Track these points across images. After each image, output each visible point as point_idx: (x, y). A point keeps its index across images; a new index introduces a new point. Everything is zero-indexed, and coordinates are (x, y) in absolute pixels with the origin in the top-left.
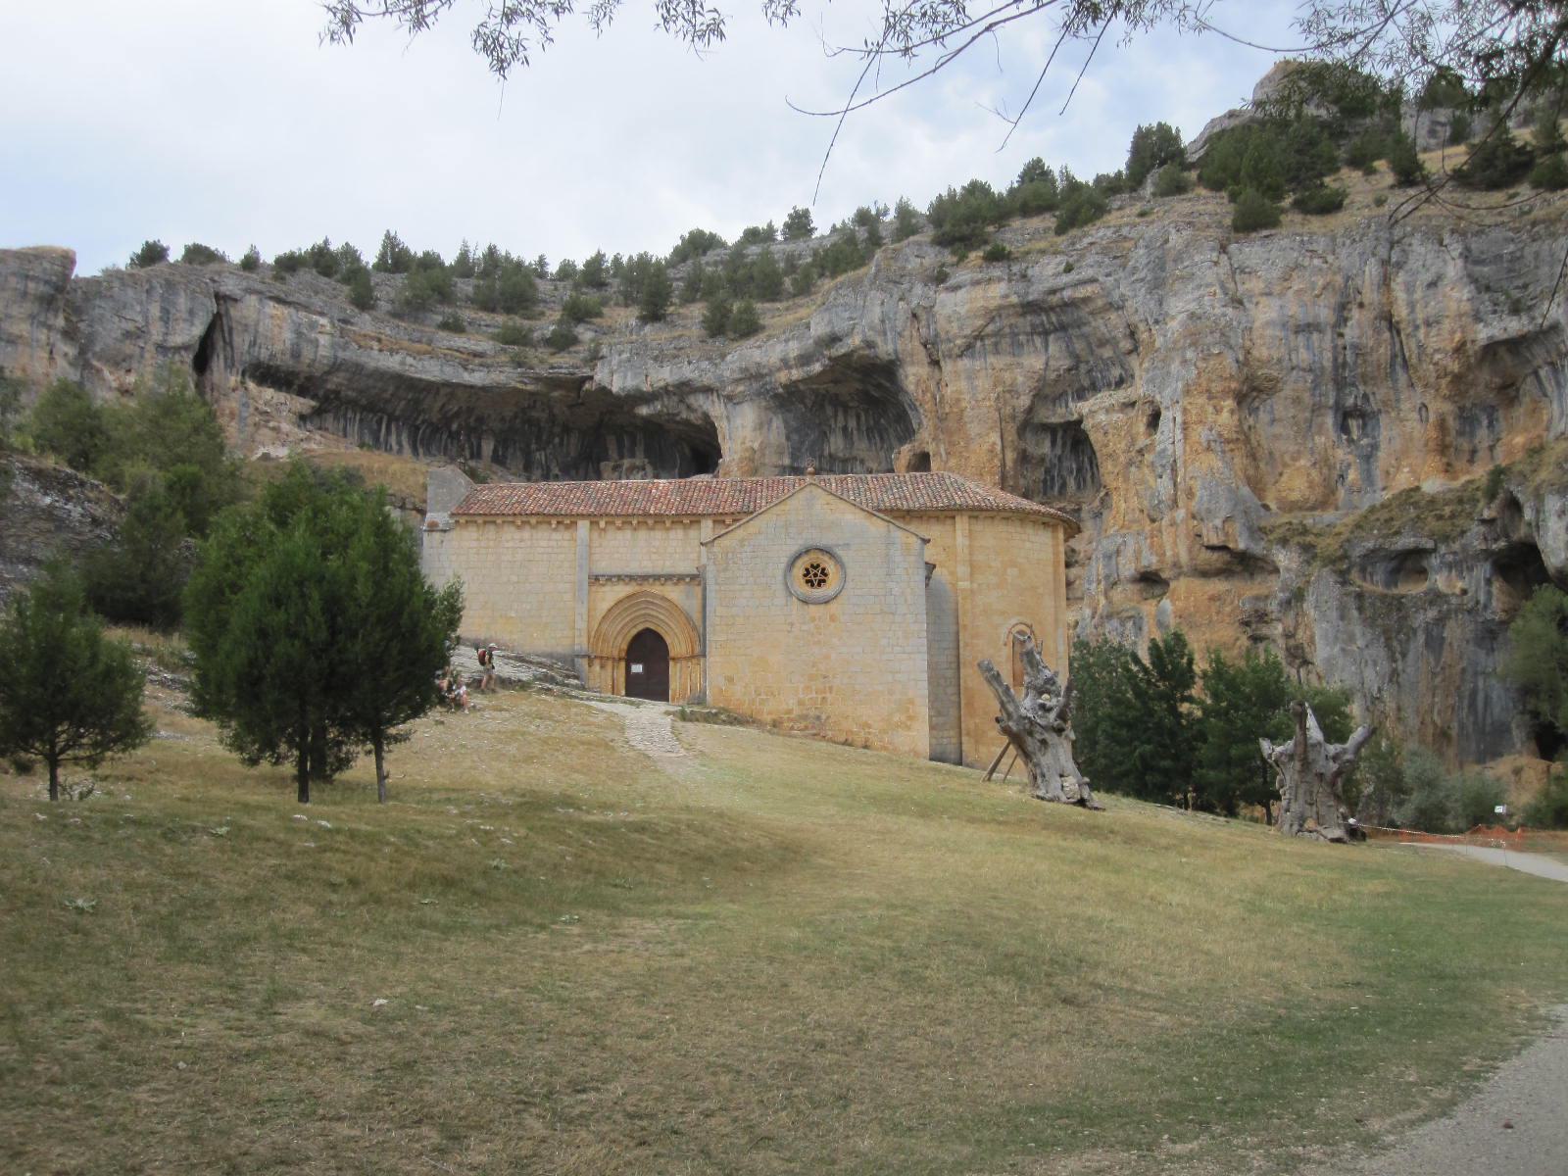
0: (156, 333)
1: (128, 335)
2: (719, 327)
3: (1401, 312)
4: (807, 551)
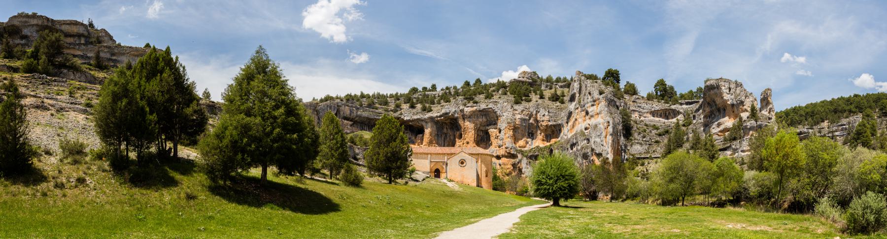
2: (424, 109)
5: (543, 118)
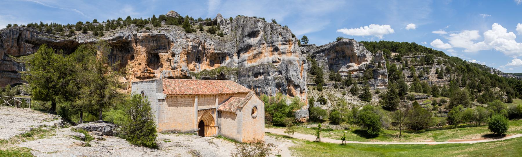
3: (206, 47)
5: (210, 47)
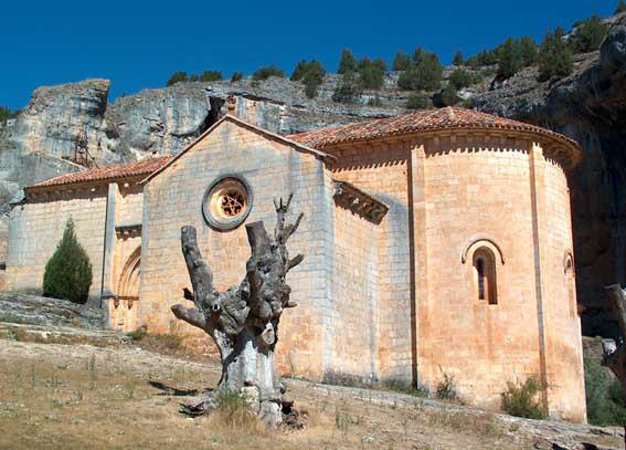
0: (170, 126)
1: (152, 129)
4: (222, 181)
